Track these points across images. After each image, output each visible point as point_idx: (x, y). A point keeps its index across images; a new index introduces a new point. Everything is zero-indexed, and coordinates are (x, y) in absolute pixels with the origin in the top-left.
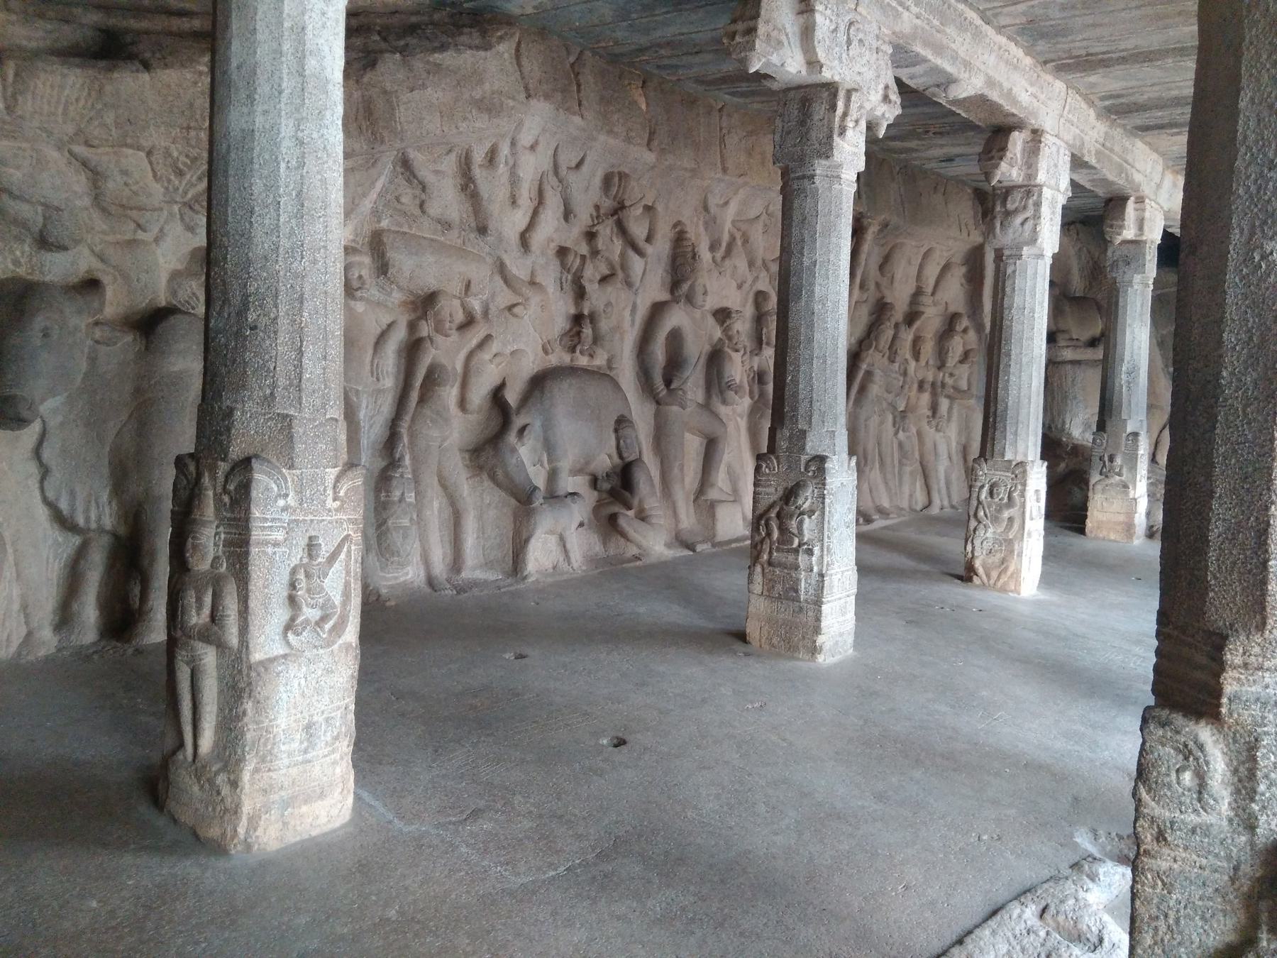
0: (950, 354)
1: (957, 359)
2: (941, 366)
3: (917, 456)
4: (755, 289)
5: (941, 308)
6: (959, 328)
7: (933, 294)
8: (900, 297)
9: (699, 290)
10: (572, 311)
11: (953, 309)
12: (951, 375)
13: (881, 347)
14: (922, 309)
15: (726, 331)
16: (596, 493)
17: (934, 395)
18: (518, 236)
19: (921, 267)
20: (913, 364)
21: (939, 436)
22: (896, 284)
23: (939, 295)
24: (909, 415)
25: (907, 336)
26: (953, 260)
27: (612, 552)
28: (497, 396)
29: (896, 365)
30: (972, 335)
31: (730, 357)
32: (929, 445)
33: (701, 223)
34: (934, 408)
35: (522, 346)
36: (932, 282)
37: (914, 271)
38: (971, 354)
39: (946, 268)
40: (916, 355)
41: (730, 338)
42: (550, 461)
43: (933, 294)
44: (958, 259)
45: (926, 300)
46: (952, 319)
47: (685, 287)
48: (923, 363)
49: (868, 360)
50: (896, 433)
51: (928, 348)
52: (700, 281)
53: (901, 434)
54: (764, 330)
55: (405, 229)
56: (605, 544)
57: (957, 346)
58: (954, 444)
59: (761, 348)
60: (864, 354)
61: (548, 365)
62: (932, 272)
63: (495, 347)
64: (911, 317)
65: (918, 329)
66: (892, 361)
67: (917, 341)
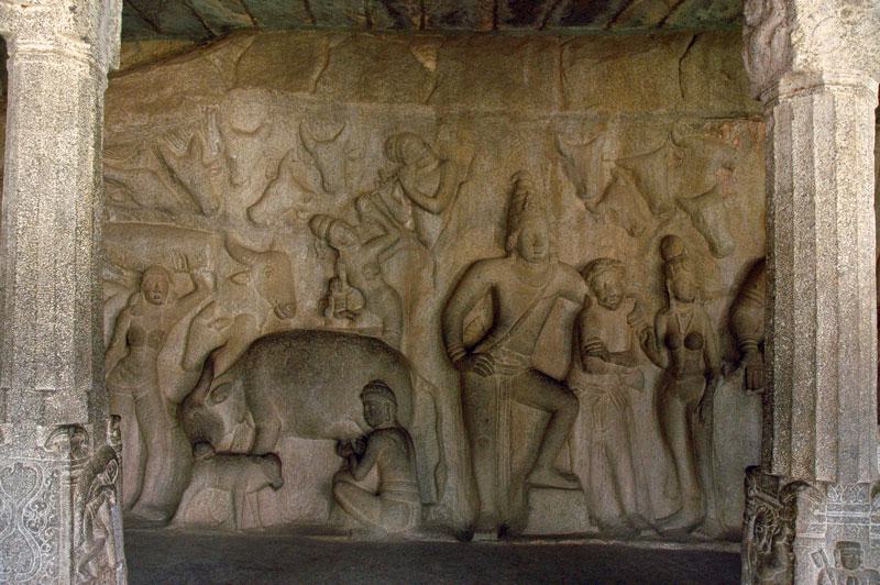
4: (662, 234)
9: (528, 241)
10: (331, 274)
15: (592, 285)
16: (341, 459)
18: (245, 210)
27: (332, 522)
28: (209, 362)
31: (594, 318)
33: (560, 168)
35: (249, 312)
41: (597, 294)
42: (255, 420)
47: (513, 239)
52: (528, 230)
54: (669, 283)
55: (134, 221)
56: (330, 513)
59: (668, 305)
61: (284, 328)
63: (218, 312)
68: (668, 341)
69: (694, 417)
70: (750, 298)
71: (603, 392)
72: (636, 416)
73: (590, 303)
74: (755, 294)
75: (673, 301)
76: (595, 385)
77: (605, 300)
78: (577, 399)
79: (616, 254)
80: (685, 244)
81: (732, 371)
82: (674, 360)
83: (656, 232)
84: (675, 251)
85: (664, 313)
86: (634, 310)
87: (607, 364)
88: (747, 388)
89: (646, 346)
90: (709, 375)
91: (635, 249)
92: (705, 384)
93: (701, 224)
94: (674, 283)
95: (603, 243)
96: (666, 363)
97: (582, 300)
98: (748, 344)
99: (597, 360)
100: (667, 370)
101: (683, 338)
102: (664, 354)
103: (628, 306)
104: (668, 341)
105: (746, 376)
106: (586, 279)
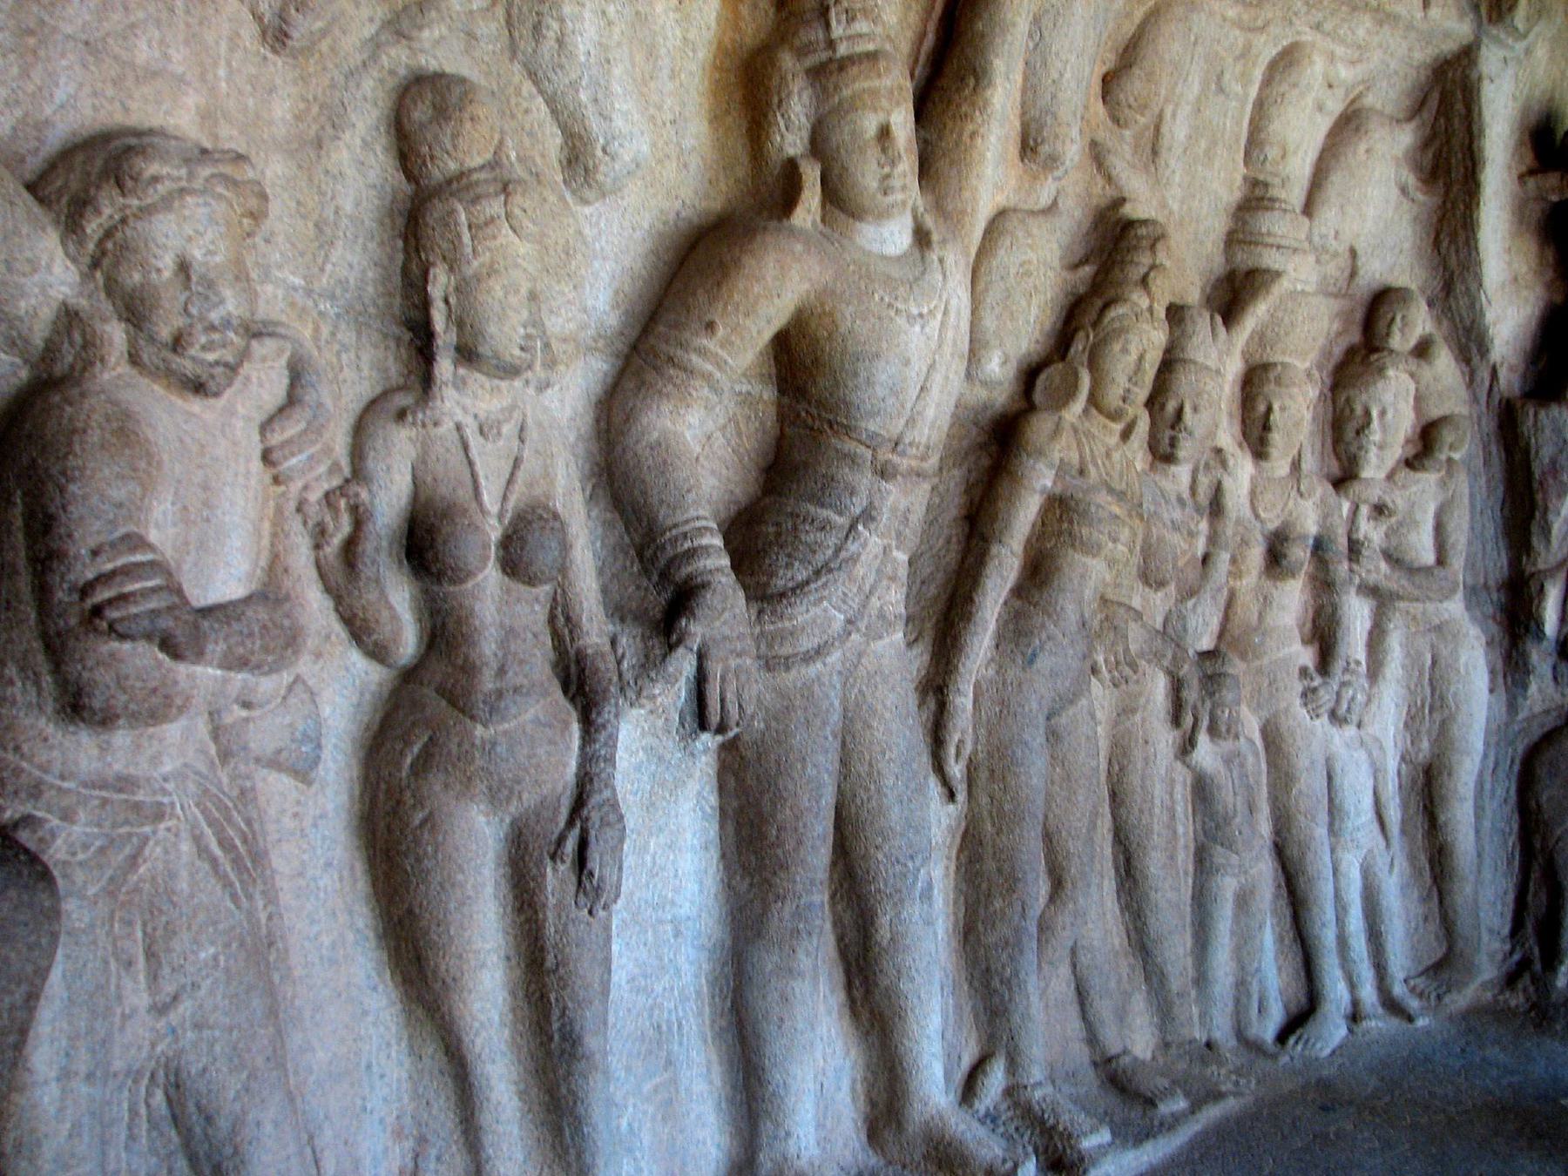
0: (1375, 434)
1: (1396, 452)
2: (1344, 479)
3: (1265, 828)
4: (399, 58)
5: (1335, 269)
6: (1400, 342)
7: (1308, 209)
8: (1187, 207)
11: (1378, 270)
12: (1380, 510)
13: (1113, 397)
14: (1271, 259)
15: (106, 261)
17: (1324, 585)
19: (1261, 110)
20: (1243, 468)
21: (1340, 739)
22: (1174, 163)
23: (1328, 216)
24: (1236, 667)
25: (1218, 359)
26: (1369, 100)
29: (1182, 473)
30: (1445, 362)
31: (125, 431)
32: (1310, 783)
34: (1323, 636)
36: (1300, 167)
37: (1233, 119)
38: (1448, 436)
39: (1349, 124)
40: (1257, 433)
41: (135, 311)
43: (1308, 209)
44: (1387, 96)
45: (1279, 225)
46: (1375, 312)
48: (1279, 466)
49: (1063, 450)
50: (1187, 747)
51: (1298, 409)
53: (1206, 753)
54: (440, 283)
57: (1394, 402)
58: (1392, 763)
60: (1039, 427)
62: (1301, 132)
64: (1233, 293)
65: (1261, 338)
66: (1162, 455)
67: (1255, 379)
68: (425, 543)
69: (556, 879)
70: (690, 371)
71: (159, 814)
72: (286, 898)
73: (90, 352)
74: (702, 352)
75: (444, 366)
76: (125, 783)
77: (178, 343)
78: (45, 876)
79: (207, 116)
80: (503, 128)
81: (650, 665)
82: (444, 633)
83: (375, 46)
84: (466, 148)
85: (401, 415)
86: (292, 400)
87: (182, 669)
88: (703, 725)
89: (344, 571)
90: (581, 686)
91: (281, 109)
92: (575, 728)
93: (549, 44)
94: (463, 289)
95: (144, 52)
96: (408, 644)
97: (39, 334)
98: (692, 554)
99: (141, 657)
100: (409, 676)
101: (495, 533)
102: (398, 601)
103: (264, 382)
104: (425, 543)
105: (701, 679)
106: (72, 226)
